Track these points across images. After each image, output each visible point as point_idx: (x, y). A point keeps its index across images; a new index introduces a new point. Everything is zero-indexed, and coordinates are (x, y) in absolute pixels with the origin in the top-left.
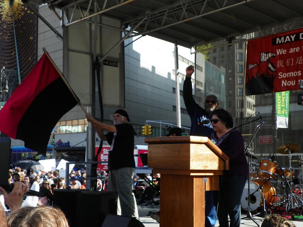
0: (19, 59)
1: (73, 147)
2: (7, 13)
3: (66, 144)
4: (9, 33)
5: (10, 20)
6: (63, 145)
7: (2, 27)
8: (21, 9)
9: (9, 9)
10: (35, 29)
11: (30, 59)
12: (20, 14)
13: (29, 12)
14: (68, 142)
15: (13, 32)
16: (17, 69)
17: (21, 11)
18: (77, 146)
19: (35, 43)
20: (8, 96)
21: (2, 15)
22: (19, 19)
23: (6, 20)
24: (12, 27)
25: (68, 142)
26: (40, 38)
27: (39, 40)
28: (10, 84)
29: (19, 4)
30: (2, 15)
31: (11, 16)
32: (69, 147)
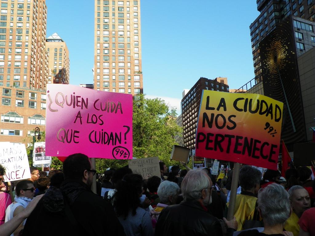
0: (287, 96)
2: (273, 67)
4: (277, 80)
5: (276, 72)
7: (271, 77)
8: (284, 62)
9: (274, 64)
11: (295, 95)
12: (283, 65)
15: (279, 79)
17: (283, 63)
23: (273, 72)
24: (278, 76)
26: (301, 78)
27: (300, 80)
29: (281, 59)
30: (270, 70)
31: (276, 69)
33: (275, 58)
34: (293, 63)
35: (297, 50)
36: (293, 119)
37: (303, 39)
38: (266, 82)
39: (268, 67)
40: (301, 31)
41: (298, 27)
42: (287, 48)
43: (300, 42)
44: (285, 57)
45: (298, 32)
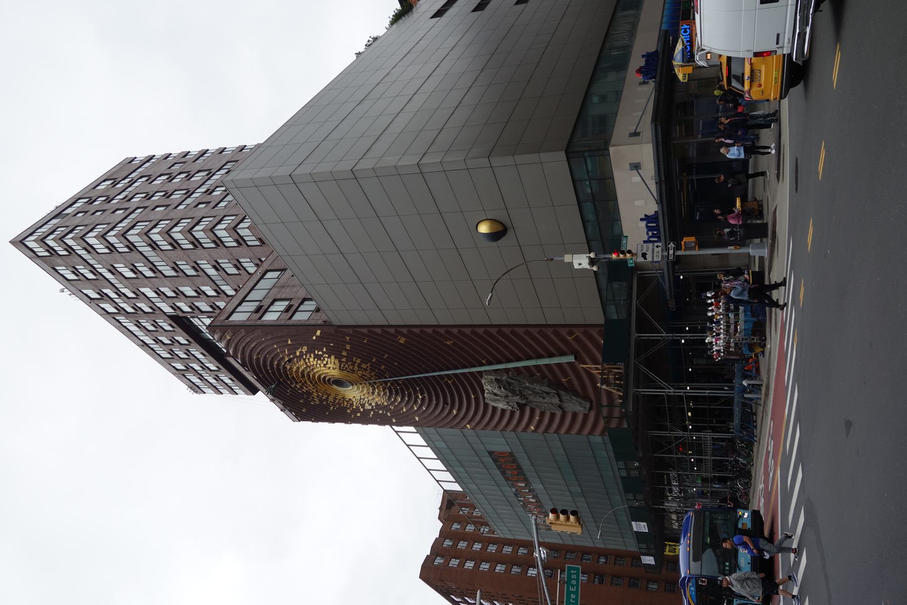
1: (660, 202)
3: (649, 228)
6: (654, 236)
10: (379, 331)
13: (348, 347)
14: (642, 220)
16: (480, 373)
18: (653, 187)
19: (409, 332)
20: (547, 393)
21: (376, 403)
22: (372, 370)
24: (392, 384)
25: (642, 220)
26: (395, 321)
28: (517, 389)
30: (376, 403)
32: (661, 218)
33: (339, 382)
34: (348, 338)
35: (313, 322)
36: (529, 358)
37: (290, 299)
38: (417, 419)
39: (368, 407)
40: (266, 304)
41: (253, 309)
42: (305, 349)
43: (293, 309)
44: (333, 357)
45: (266, 311)
